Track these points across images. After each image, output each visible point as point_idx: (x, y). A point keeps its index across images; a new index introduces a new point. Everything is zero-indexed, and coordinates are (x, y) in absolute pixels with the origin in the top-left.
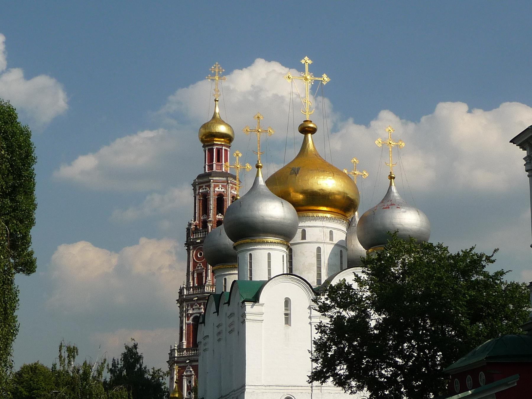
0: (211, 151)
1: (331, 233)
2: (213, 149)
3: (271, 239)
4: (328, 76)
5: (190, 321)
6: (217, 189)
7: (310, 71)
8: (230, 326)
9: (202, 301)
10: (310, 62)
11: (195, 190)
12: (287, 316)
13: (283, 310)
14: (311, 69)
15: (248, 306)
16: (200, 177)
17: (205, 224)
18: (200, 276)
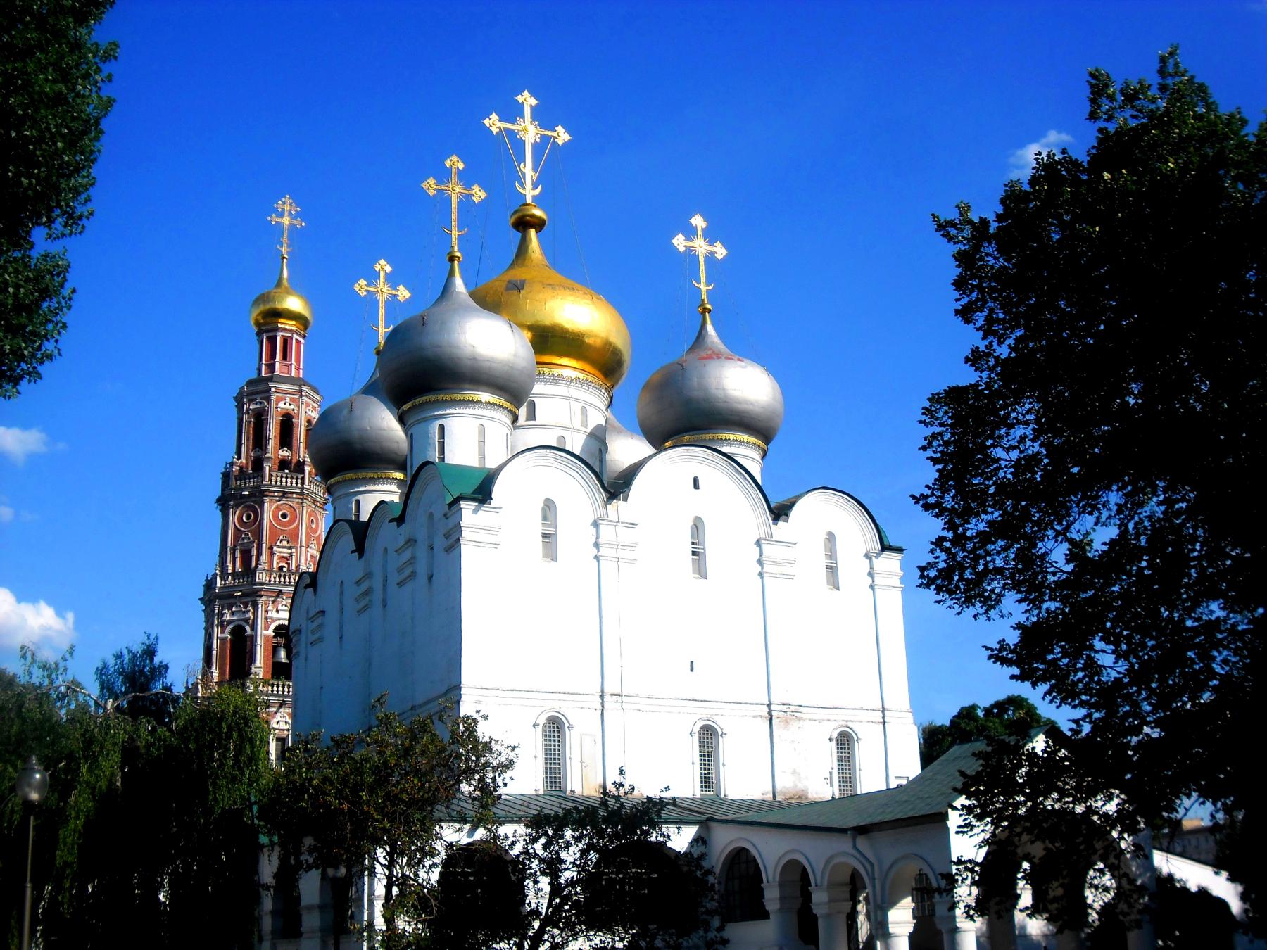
0: (272, 341)
1: (584, 410)
2: (276, 337)
3: (485, 396)
5: (227, 635)
6: (281, 405)
7: (534, 118)
8: (400, 570)
9: (249, 599)
11: (240, 407)
12: (548, 537)
13: (538, 528)
15: (467, 508)
16: (250, 383)
17: (258, 465)
18: (246, 555)
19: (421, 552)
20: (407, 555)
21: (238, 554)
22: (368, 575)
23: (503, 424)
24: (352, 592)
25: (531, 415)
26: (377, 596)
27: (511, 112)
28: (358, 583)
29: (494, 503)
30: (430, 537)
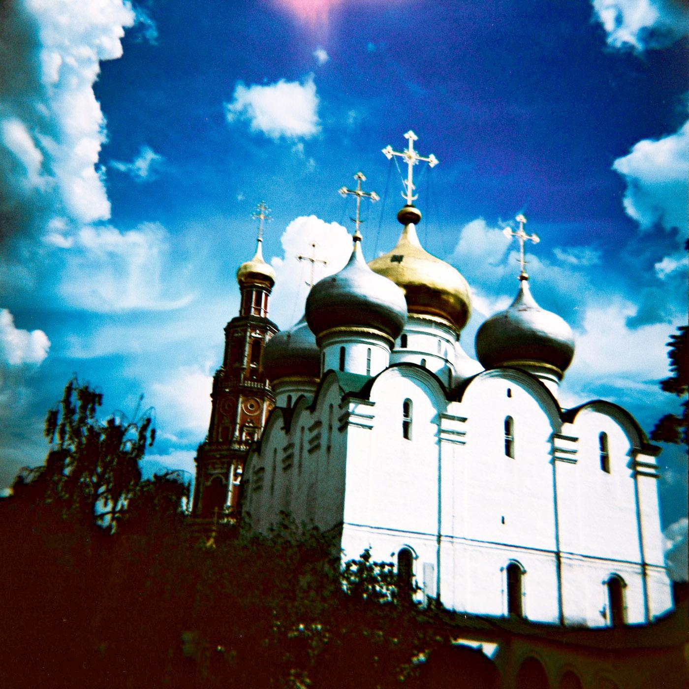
4: (437, 157)
8: (311, 442)
9: (225, 460)
10: (415, 138)
12: (406, 426)
14: (417, 146)
16: (235, 320)
19: (324, 430)
20: (315, 432)
21: (220, 430)
22: (291, 445)
23: (384, 348)
24: (281, 455)
25: (404, 344)
26: (296, 460)
27: (402, 145)
28: (285, 449)
29: (371, 399)
30: (330, 420)
